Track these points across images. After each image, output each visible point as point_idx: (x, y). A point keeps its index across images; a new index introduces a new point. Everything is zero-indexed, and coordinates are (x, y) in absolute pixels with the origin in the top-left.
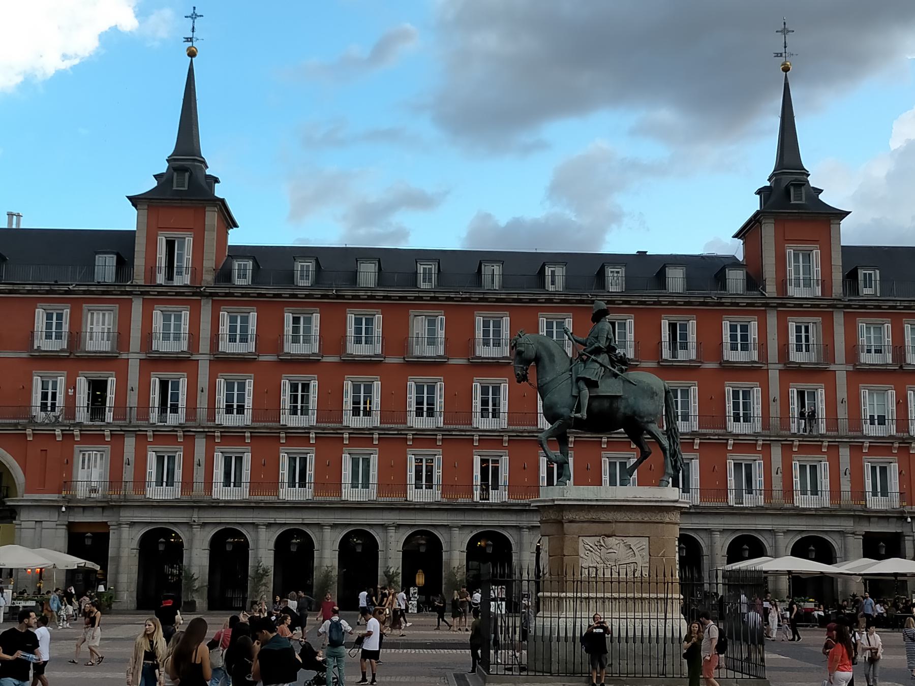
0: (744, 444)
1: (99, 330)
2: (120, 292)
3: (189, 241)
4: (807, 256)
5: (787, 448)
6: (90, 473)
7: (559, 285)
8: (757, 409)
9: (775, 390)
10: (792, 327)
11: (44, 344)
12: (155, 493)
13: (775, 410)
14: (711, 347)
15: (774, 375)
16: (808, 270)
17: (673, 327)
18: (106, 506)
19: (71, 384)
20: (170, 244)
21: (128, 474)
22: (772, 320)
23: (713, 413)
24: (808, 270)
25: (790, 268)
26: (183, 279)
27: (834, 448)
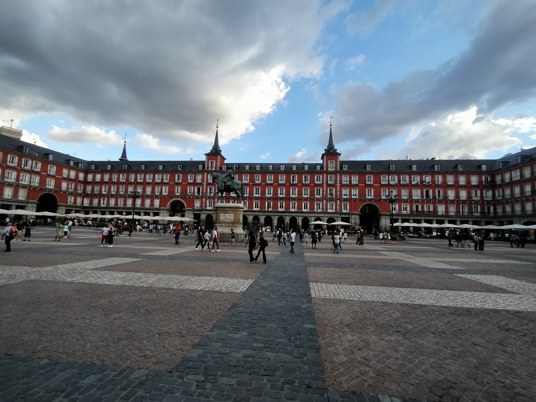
0: (318, 200)
1: (199, 179)
2: (202, 172)
3: (215, 162)
4: (333, 163)
5: (327, 201)
6: (197, 204)
7: (284, 169)
8: (321, 193)
9: (325, 189)
10: (329, 176)
11: (190, 181)
12: (208, 208)
13: (325, 193)
14: (312, 180)
15: (325, 186)
16: (332, 165)
17: (305, 177)
18: (200, 210)
19: (194, 188)
20: (212, 163)
21: (204, 204)
22: (325, 175)
23: (312, 194)
24: (332, 165)
25: (329, 165)
26: (214, 169)
27: (336, 200)
